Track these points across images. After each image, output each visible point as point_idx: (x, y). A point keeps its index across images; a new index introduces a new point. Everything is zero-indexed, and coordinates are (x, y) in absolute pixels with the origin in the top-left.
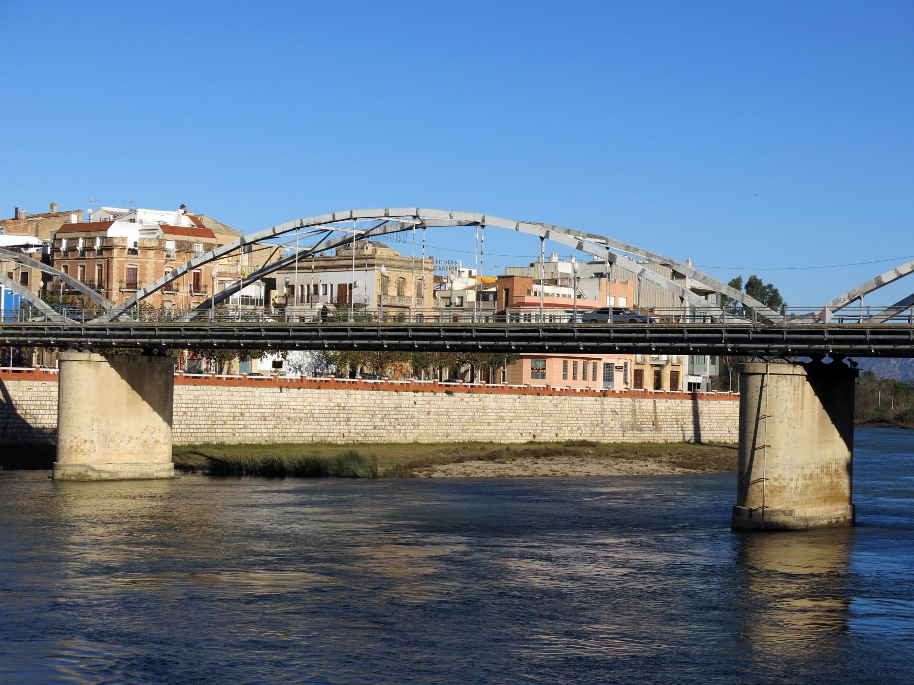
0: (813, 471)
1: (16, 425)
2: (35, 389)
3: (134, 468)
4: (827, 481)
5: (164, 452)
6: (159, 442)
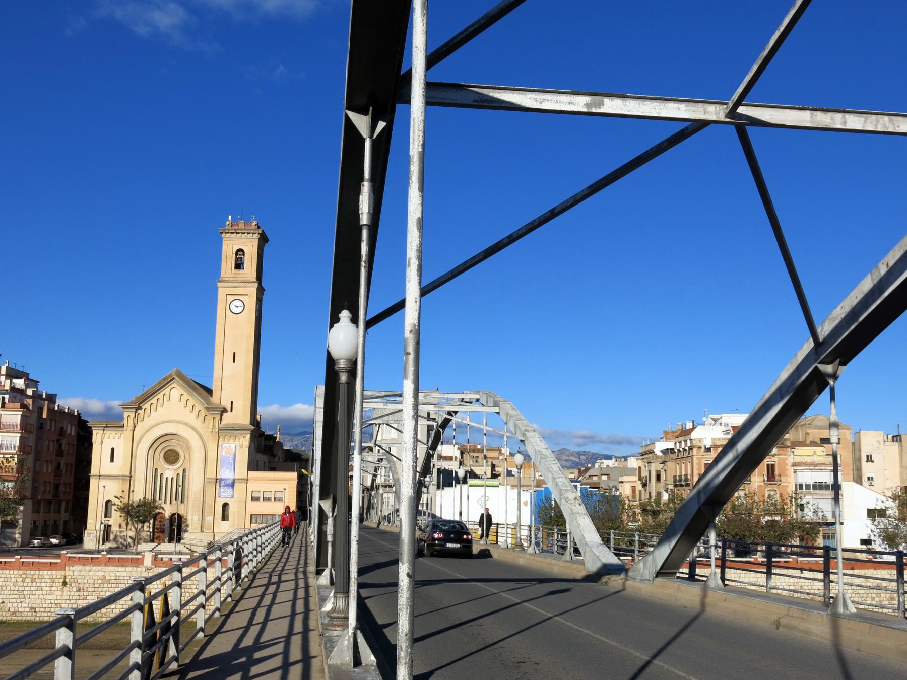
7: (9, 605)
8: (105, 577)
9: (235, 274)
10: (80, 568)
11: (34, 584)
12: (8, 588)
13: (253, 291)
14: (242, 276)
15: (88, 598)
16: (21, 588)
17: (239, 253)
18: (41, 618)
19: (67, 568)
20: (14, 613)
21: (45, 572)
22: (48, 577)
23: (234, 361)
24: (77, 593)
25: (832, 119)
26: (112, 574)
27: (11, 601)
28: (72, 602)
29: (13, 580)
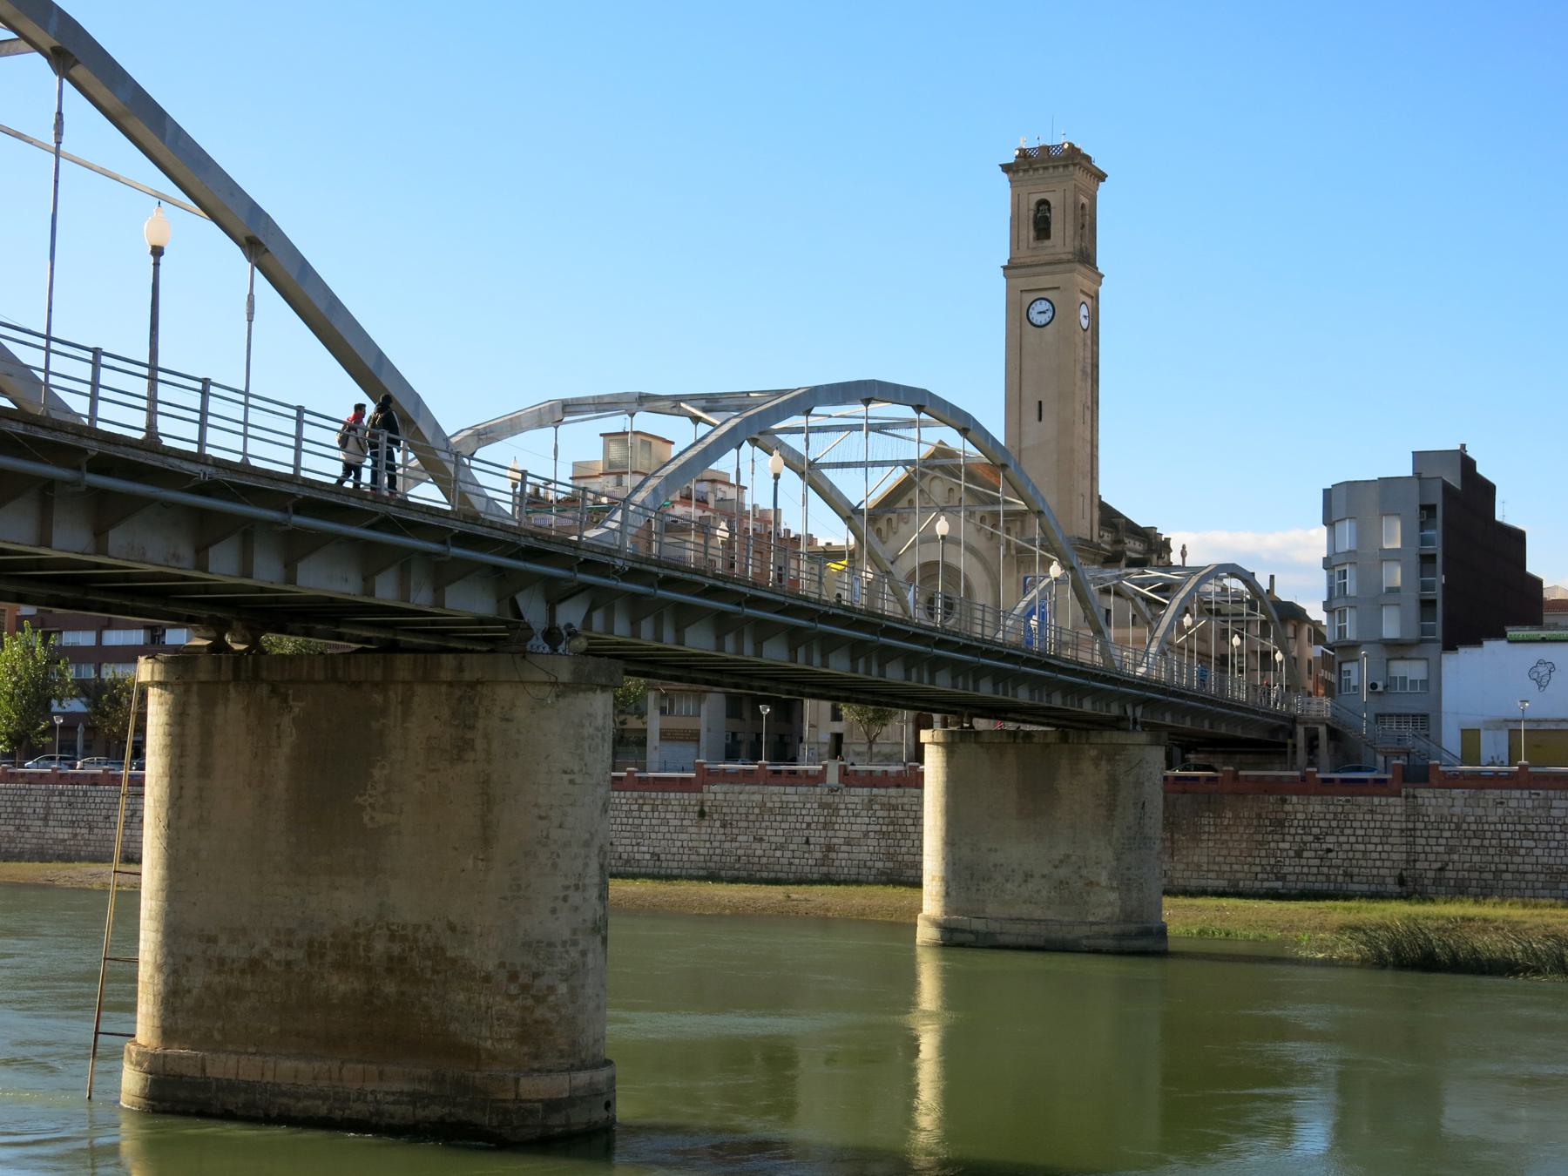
0: (267, 954)
1: (1467, 866)
2: (1513, 803)
3: (1032, 929)
4: (342, 988)
5: (1111, 904)
6: (1098, 884)
7: (620, 849)
8: (764, 803)
9: (1035, 248)
10: (725, 787)
11: (656, 814)
12: (618, 820)
15: (740, 838)
16: (636, 822)
18: (669, 871)
19: (705, 787)
20: (628, 861)
21: (672, 795)
22: (677, 803)
23: (1040, 419)
24: (722, 830)
26: (775, 798)
27: (624, 841)
28: (717, 844)
29: (625, 808)
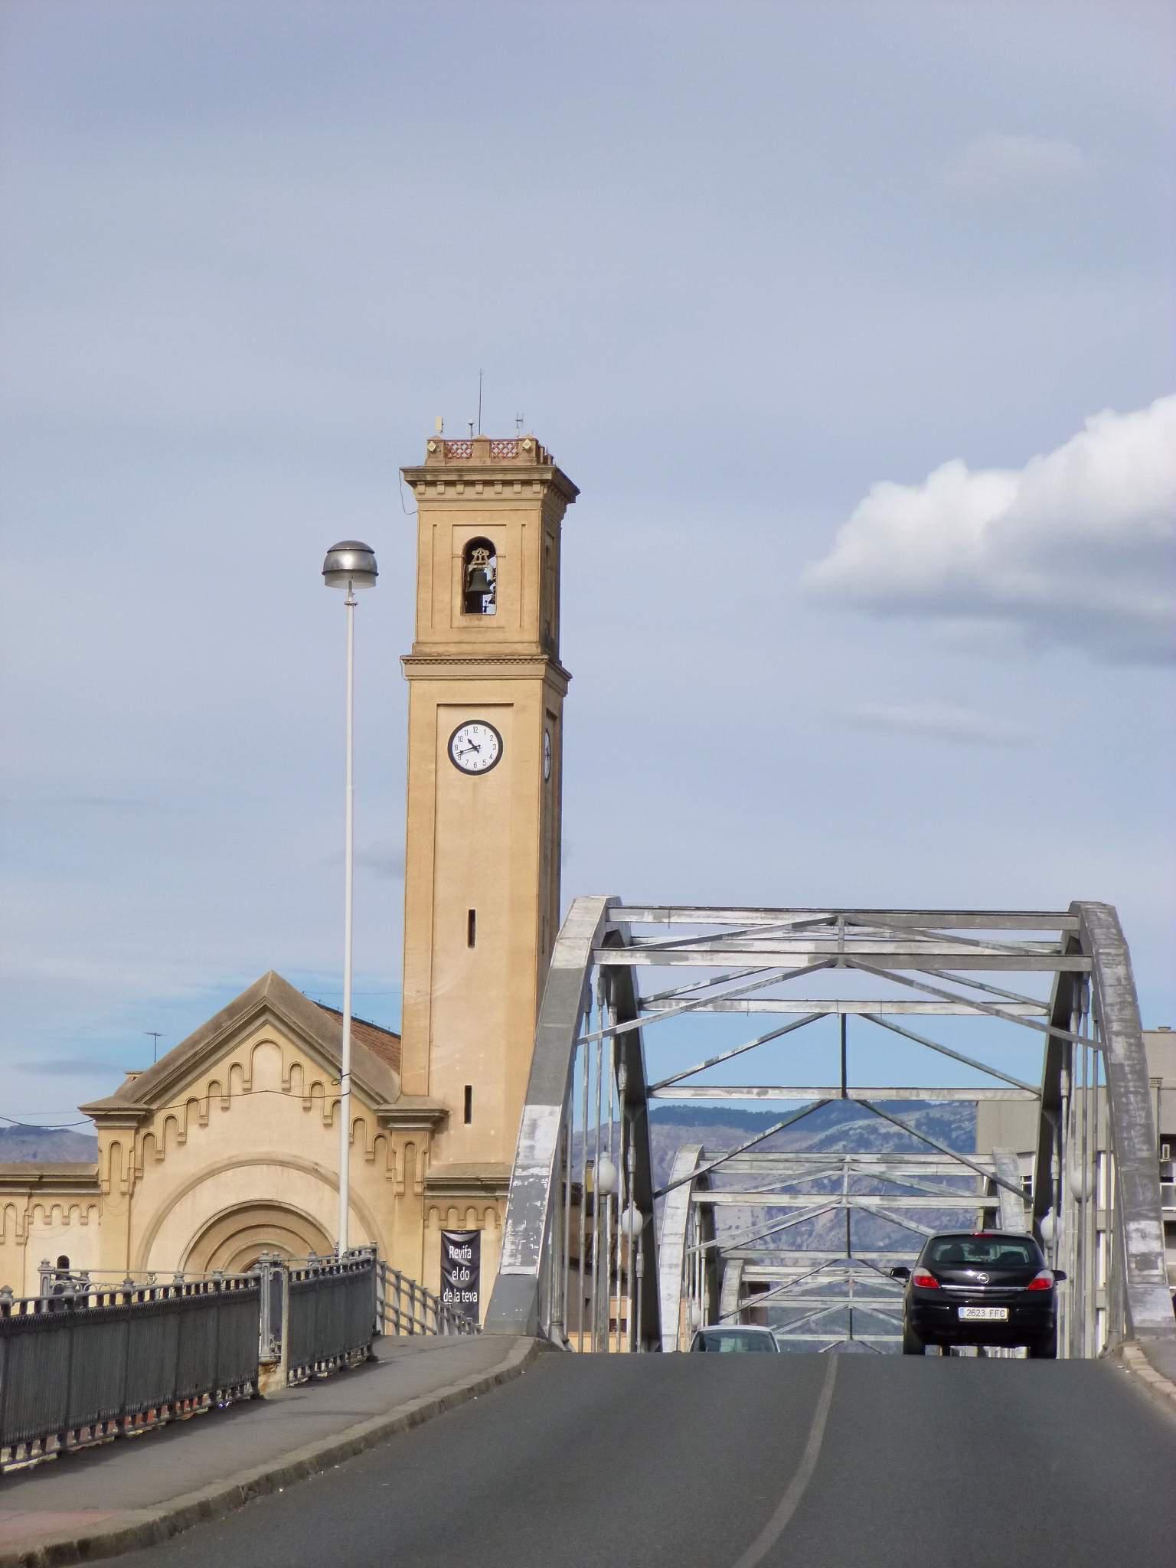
13: (529, 692)
14: (490, 636)
17: (475, 553)
23: (471, 942)
25: (911, 1094)
